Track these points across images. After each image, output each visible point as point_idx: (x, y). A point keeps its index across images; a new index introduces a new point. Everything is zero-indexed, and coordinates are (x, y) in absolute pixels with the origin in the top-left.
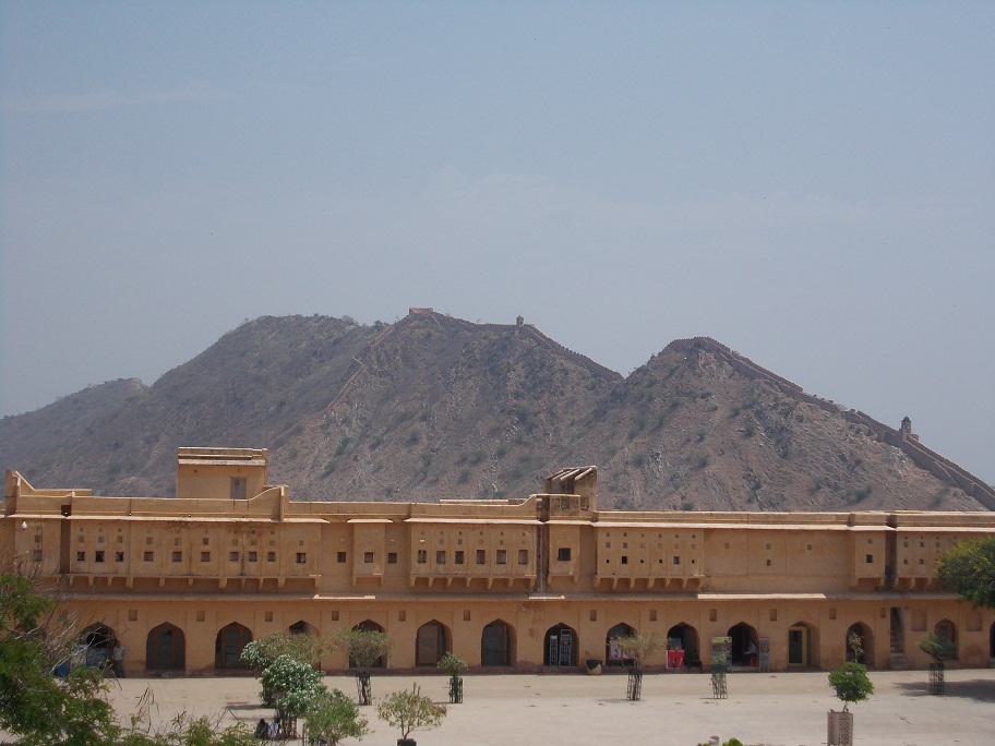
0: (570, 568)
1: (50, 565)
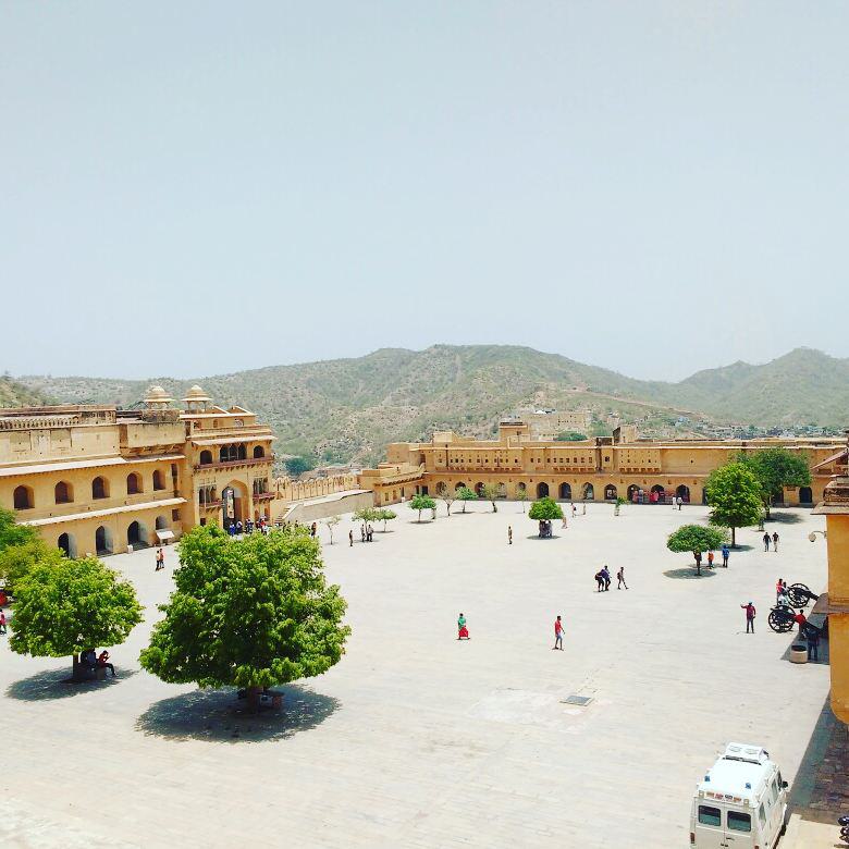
0: (610, 464)
1: (444, 464)
